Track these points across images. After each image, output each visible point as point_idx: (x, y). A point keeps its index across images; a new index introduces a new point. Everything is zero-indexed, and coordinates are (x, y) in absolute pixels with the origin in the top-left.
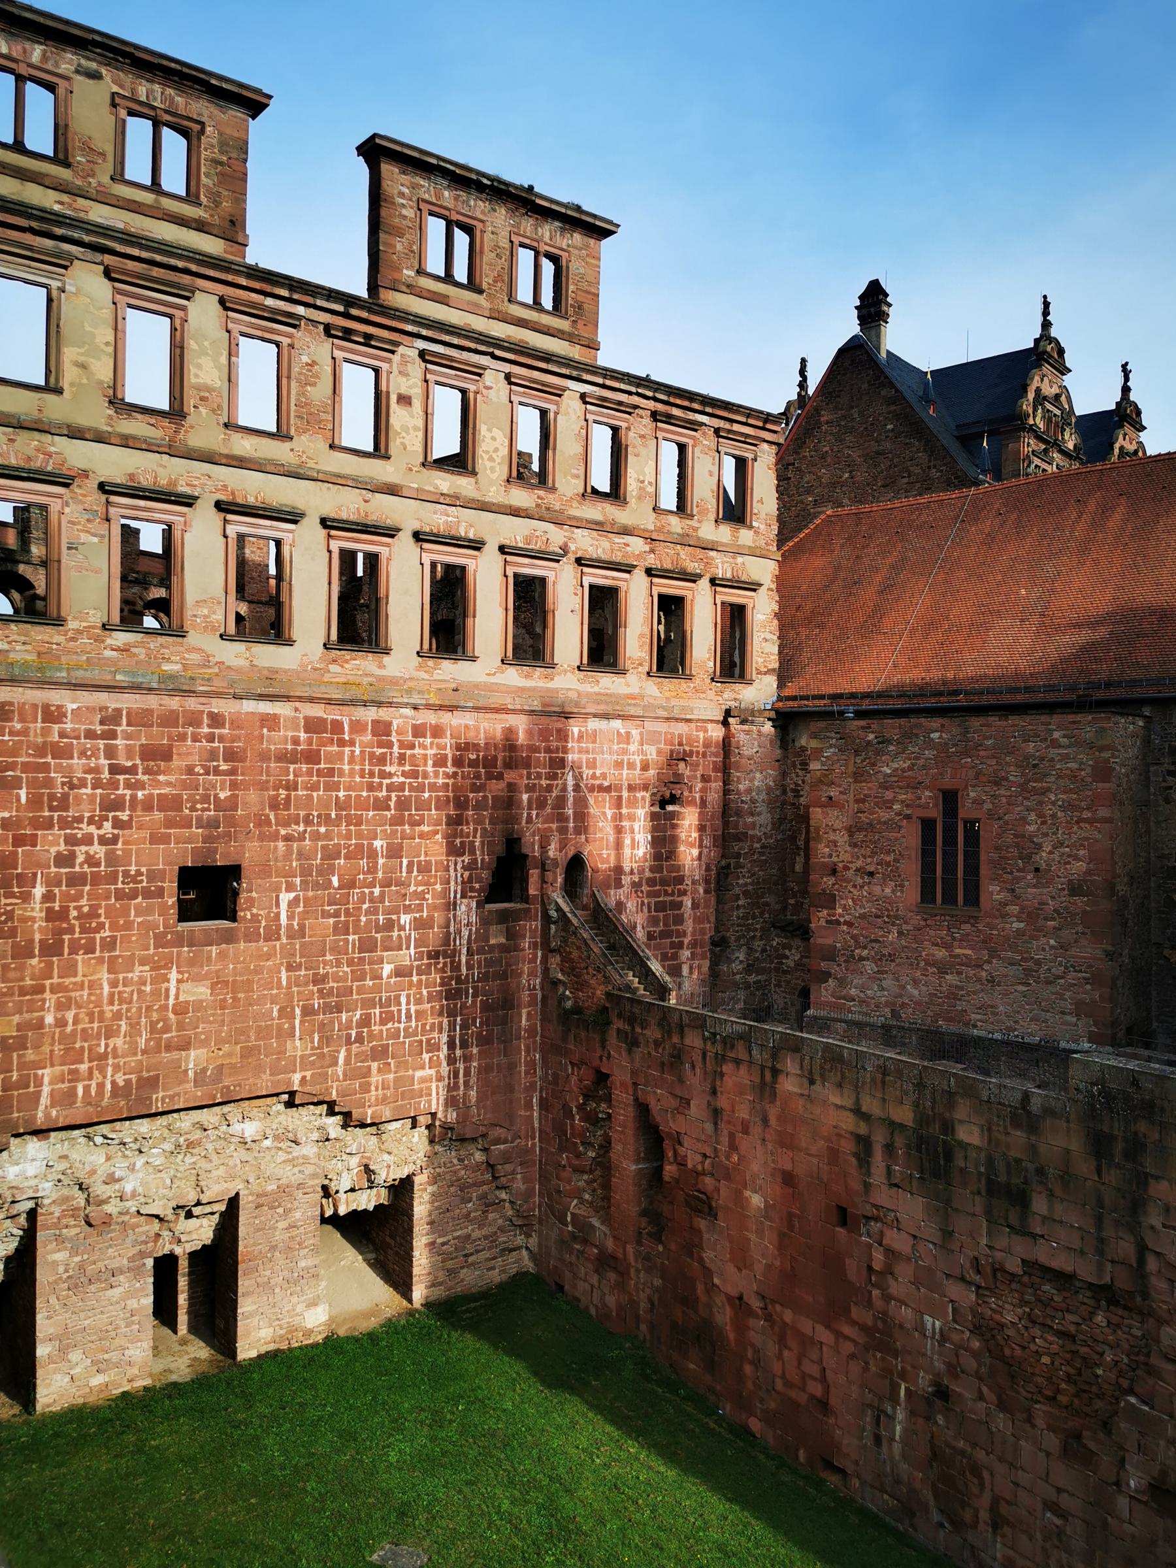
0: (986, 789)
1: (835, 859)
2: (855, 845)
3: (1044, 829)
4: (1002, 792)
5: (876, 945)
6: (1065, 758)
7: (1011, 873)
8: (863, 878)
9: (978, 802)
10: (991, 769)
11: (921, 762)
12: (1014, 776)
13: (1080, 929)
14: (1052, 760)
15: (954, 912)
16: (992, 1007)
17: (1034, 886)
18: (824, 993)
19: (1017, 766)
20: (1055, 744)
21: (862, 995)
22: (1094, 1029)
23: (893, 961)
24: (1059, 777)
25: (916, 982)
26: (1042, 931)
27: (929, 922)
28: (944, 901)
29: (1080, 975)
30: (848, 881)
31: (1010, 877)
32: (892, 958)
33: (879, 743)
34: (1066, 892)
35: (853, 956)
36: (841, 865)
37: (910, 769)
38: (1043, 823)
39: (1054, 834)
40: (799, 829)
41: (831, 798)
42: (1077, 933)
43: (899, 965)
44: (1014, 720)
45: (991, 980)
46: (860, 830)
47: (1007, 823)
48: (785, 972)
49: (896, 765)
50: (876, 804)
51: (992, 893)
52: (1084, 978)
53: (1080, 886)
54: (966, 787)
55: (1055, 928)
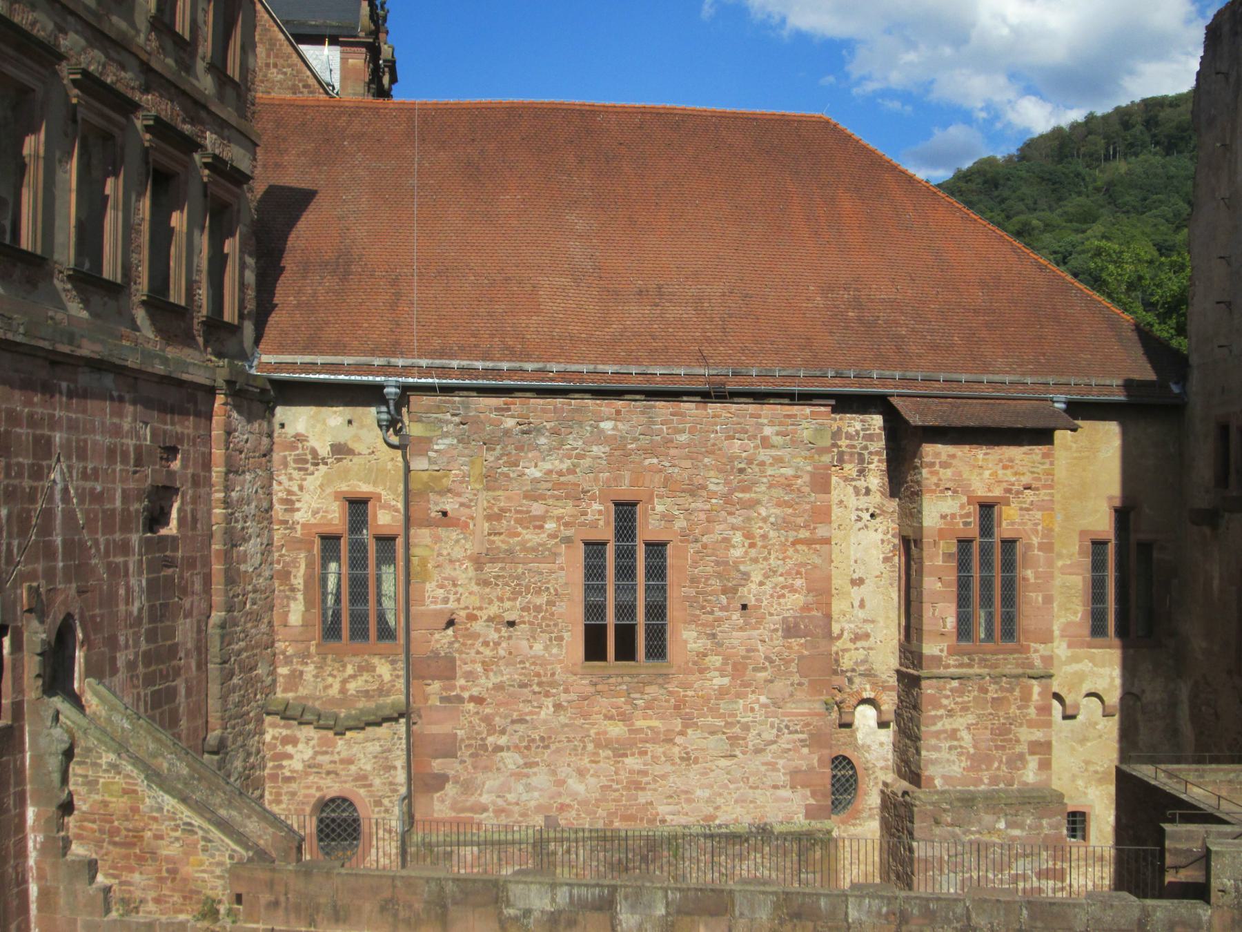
0: (680, 501)
1: (451, 605)
2: (486, 583)
3: (753, 553)
4: (700, 505)
5: (521, 728)
6: (779, 461)
7: (712, 612)
8: (498, 630)
9: (668, 518)
10: (685, 475)
11: (586, 462)
12: (716, 484)
13: (796, 679)
14: (762, 464)
15: (633, 671)
16: (687, 792)
17: (741, 629)
18: (437, 806)
19: (720, 471)
20: (766, 443)
21: (500, 802)
22: (812, 801)
23: (547, 747)
24: (770, 486)
25: (581, 773)
26: (749, 685)
27: (599, 687)
28: (619, 657)
29: (796, 736)
30: (476, 636)
31: (711, 617)
32: (545, 742)
33: (524, 432)
34: (780, 633)
35: (484, 747)
36: (463, 613)
37: (571, 471)
38: (752, 545)
39: (765, 559)
40: (294, 561)
41: (445, 514)
42: (792, 685)
43: (558, 751)
44: (714, 408)
45: (686, 758)
46: (493, 561)
47: (705, 546)
48: (288, 780)
49: (547, 466)
50: (518, 521)
51: (686, 642)
52: (802, 741)
53: (796, 625)
54: (651, 500)
55: (766, 681)
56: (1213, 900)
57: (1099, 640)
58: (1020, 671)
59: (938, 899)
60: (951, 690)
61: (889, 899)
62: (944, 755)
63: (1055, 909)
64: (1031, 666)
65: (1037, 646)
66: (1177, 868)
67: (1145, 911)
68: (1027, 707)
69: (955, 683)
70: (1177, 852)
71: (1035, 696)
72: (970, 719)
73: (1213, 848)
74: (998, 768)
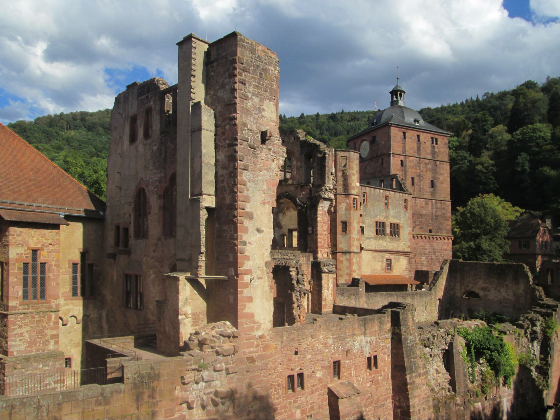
56: (125, 382)
57: (75, 297)
58: (47, 310)
59: (27, 397)
60: (20, 318)
61: (6, 401)
62: (18, 343)
63: (72, 394)
64: (52, 308)
65: (54, 300)
66: (111, 373)
67: (102, 389)
68: (50, 322)
69: (22, 316)
70: (111, 368)
71: (53, 318)
72: (28, 328)
73: (125, 365)
74: (39, 346)
